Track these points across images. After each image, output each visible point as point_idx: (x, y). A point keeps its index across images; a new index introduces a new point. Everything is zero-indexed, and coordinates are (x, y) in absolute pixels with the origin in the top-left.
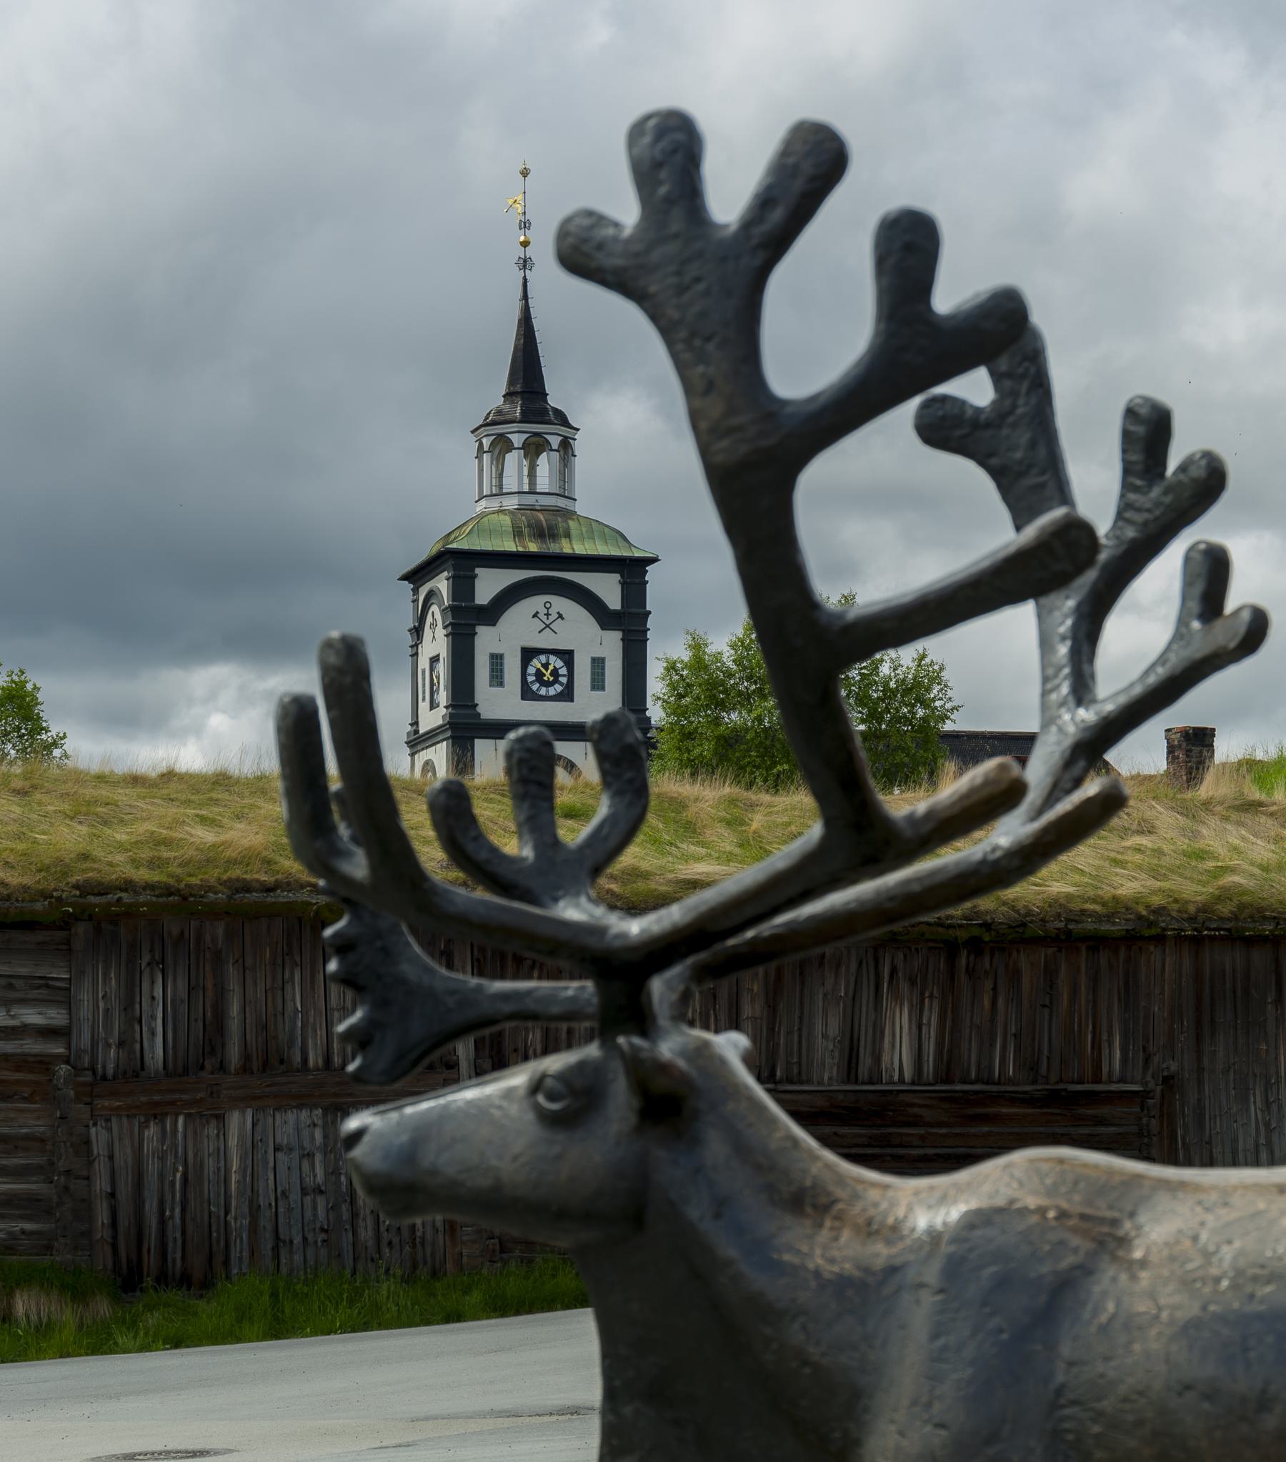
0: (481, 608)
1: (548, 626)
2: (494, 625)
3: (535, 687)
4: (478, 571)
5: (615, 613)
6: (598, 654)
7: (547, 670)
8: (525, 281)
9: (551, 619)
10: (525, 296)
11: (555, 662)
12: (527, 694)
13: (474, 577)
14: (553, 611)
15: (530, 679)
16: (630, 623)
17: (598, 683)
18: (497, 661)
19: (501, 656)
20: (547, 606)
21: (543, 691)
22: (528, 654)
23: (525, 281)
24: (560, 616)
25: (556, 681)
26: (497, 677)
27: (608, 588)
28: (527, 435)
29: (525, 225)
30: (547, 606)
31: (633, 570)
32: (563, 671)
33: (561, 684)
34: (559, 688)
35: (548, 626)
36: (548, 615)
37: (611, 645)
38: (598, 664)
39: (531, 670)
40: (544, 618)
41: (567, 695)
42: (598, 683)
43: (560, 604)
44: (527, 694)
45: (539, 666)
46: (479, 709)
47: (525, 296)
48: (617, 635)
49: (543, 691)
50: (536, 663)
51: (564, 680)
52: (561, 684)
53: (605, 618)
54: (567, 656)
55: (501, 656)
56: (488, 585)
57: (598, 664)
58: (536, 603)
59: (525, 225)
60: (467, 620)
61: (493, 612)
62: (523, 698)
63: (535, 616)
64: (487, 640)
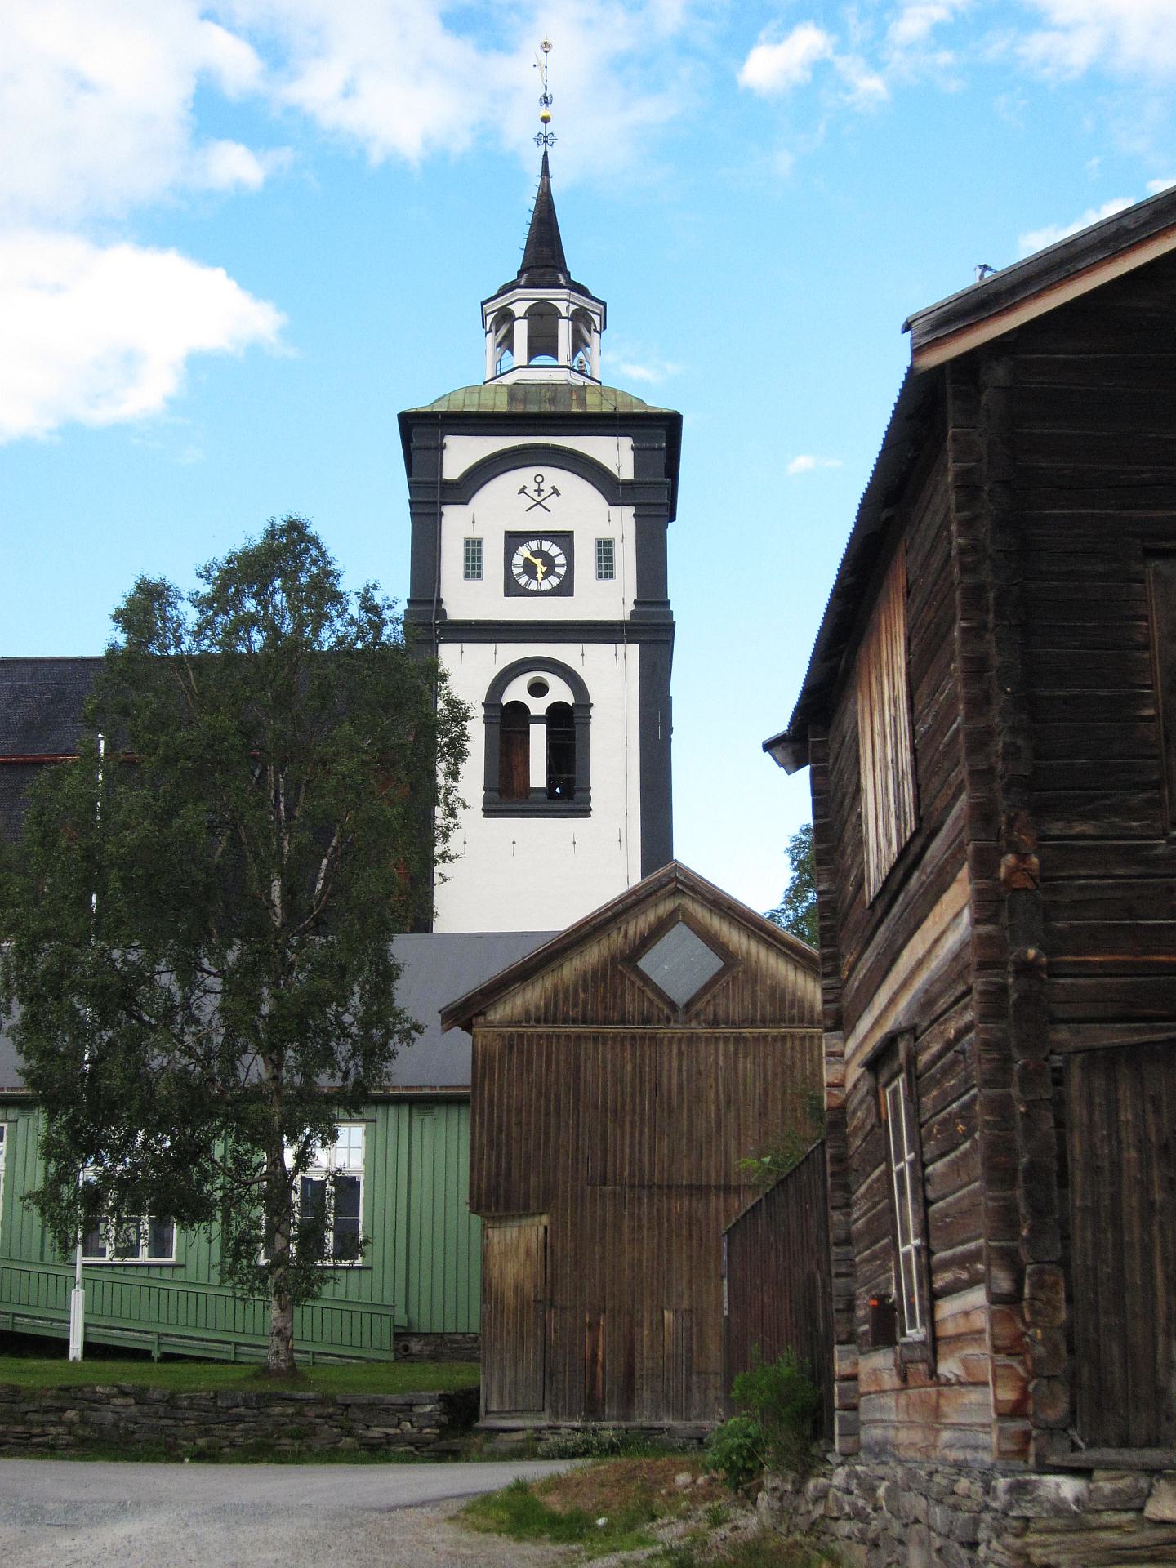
1: (539, 503)
3: (523, 581)
4: (449, 440)
5: (626, 483)
6: (605, 535)
7: (540, 554)
12: (512, 588)
13: (443, 447)
14: (546, 487)
15: (516, 571)
17: (605, 569)
18: (474, 548)
19: (480, 542)
20: (539, 481)
22: (514, 539)
24: (556, 492)
26: (473, 568)
27: (616, 454)
30: (539, 481)
32: (561, 559)
33: (558, 576)
34: (554, 581)
35: (539, 503)
36: (539, 491)
37: (622, 524)
38: (605, 549)
39: (517, 560)
41: (565, 588)
42: (605, 569)
44: (512, 588)
45: (527, 554)
48: (631, 510)
50: (524, 551)
51: (561, 571)
52: (558, 576)
54: (564, 539)
55: (480, 542)
56: (460, 454)
57: (605, 549)
59: (546, 100)
60: (431, 496)
62: (506, 595)
63: (522, 491)
64: (456, 523)
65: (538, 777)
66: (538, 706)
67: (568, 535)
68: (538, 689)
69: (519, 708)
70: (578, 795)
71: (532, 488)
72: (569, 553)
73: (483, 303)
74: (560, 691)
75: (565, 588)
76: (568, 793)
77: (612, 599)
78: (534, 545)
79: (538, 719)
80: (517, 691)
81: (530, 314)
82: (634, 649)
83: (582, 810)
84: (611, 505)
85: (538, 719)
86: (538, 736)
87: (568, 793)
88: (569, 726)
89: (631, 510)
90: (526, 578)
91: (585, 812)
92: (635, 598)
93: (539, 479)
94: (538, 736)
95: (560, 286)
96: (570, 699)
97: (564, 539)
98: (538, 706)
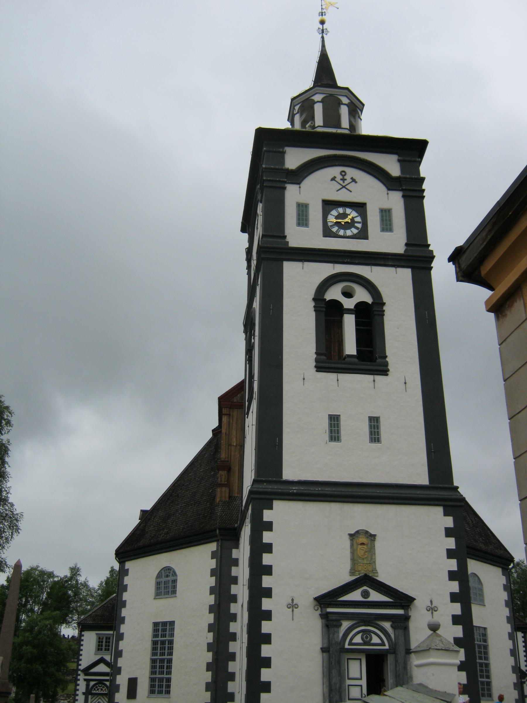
1: (344, 187)
6: (386, 206)
8: (323, 38)
9: (346, 182)
10: (323, 46)
11: (352, 214)
12: (327, 233)
13: (284, 153)
14: (348, 178)
16: (411, 188)
18: (303, 210)
19: (306, 206)
20: (343, 174)
21: (341, 232)
22: (329, 205)
23: (323, 38)
24: (353, 180)
26: (303, 219)
27: (391, 164)
28: (324, 95)
29: (322, 14)
30: (343, 174)
31: (412, 150)
33: (357, 228)
34: (355, 231)
36: (343, 180)
37: (396, 202)
38: (386, 215)
40: (341, 182)
41: (363, 234)
43: (351, 172)
44: (327, 233)
46: (288, 239)
47: (323, 46)
49: (341, 232)
50: (334, 213)
51: (359, 226)
52: (357, 228)
53: (390, 182)
56: (294, 158)
57: (386, 215)
58: (335, 171)
61: (298, 175)
63: (333, 179)
64: (293, 195)
65: (350, 347)
66: (349, 304)
68: (348, 294)
69: (336, 305)
70: (379, 360)
71: (339, 178)
74: (362, 295)
76: (371, 359)
77: (395, 242)
78: (341, 210)
79: (349, 311)
80: (334, 293)
83: (384, 371)
85: (349, 311)
86: (349, 322)
87: (371, 359)
88: (370, 317)
91: (329, 415)
94: (349, 322)
96: (369, 300)
98: (349, 304)
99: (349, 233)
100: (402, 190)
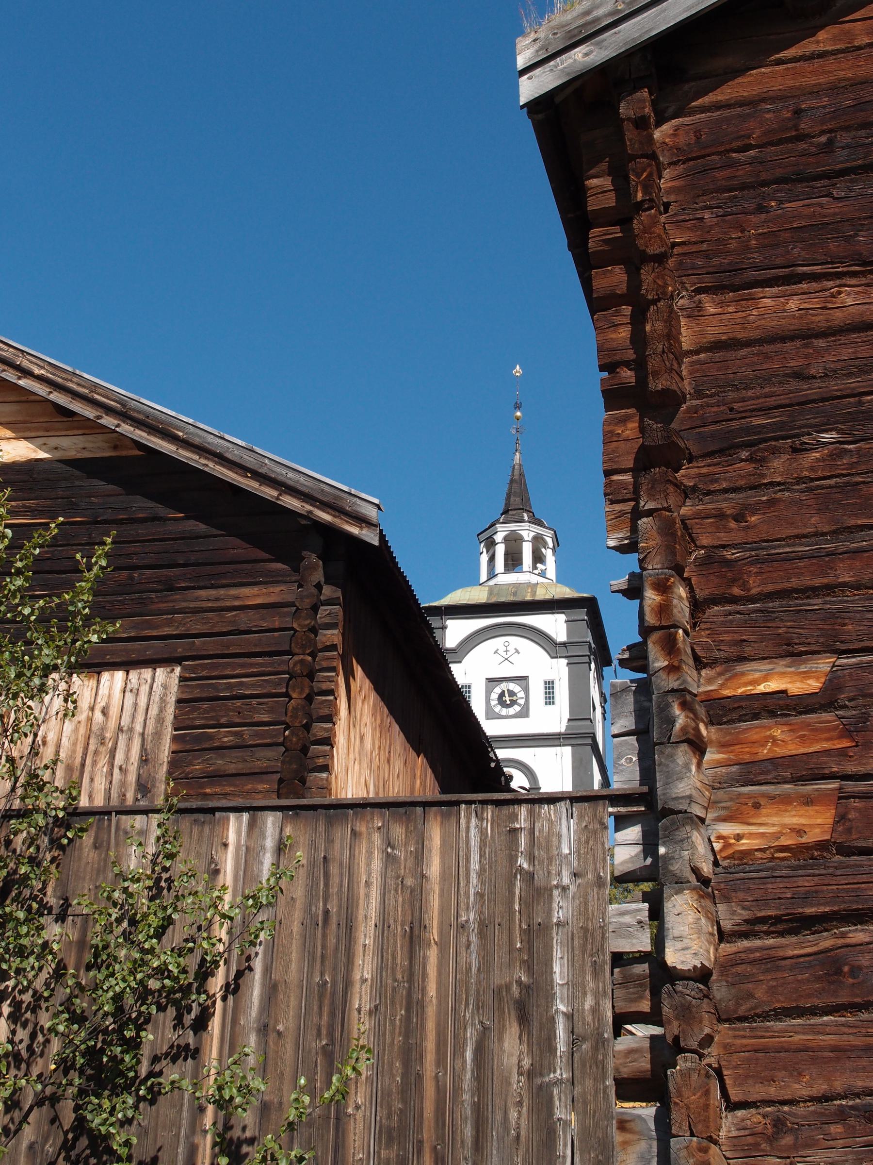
0: (453, 651)
2: (460, 662)
5: (564, 644)
6: (549, 678)
17: (550, 699)
21: (504, 711)
22: (492, 682)
24: (517, 651)
25: (513, 703)
27: (555, 625)
32: (521, 694)
33: (519, 705)
36: (507, 651)
38: (549, 686)
40: (504, 654)
41: (524, 713)
42: (550, 699)
43: (515, 642)
48: (564, 661)
50: (498, 690)
51: (522, 702)
52: (519, 705)
57: (549, 686)
63: (496, 652)
67: (525, 678)
72: (526, 690)
73: (478, 535)
75: (524, 713)
81: (506, 540)
82: (567, 751)
84: (552, 658)
89: (564, 661)
90: (499, 707)
92: (568, 717)
93: (506, 644)
95: (524, 521)
97: (522, 680)
99: (512, 711)
100: (566, 657)
